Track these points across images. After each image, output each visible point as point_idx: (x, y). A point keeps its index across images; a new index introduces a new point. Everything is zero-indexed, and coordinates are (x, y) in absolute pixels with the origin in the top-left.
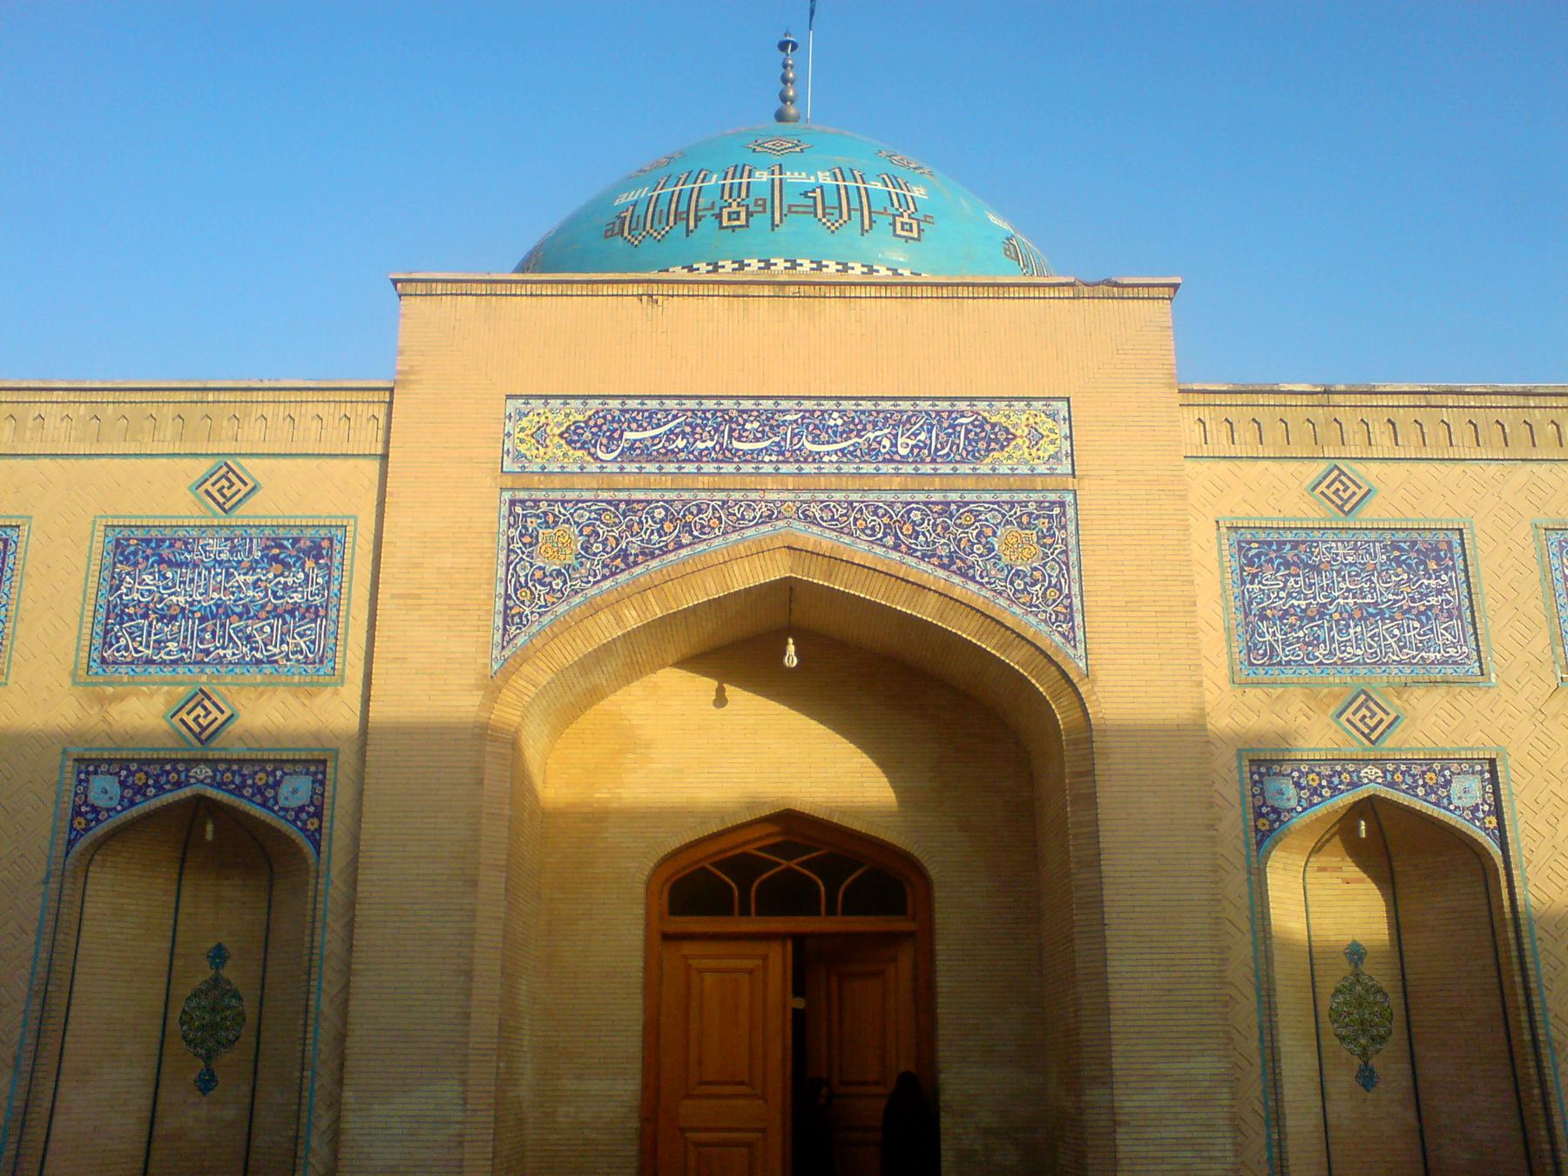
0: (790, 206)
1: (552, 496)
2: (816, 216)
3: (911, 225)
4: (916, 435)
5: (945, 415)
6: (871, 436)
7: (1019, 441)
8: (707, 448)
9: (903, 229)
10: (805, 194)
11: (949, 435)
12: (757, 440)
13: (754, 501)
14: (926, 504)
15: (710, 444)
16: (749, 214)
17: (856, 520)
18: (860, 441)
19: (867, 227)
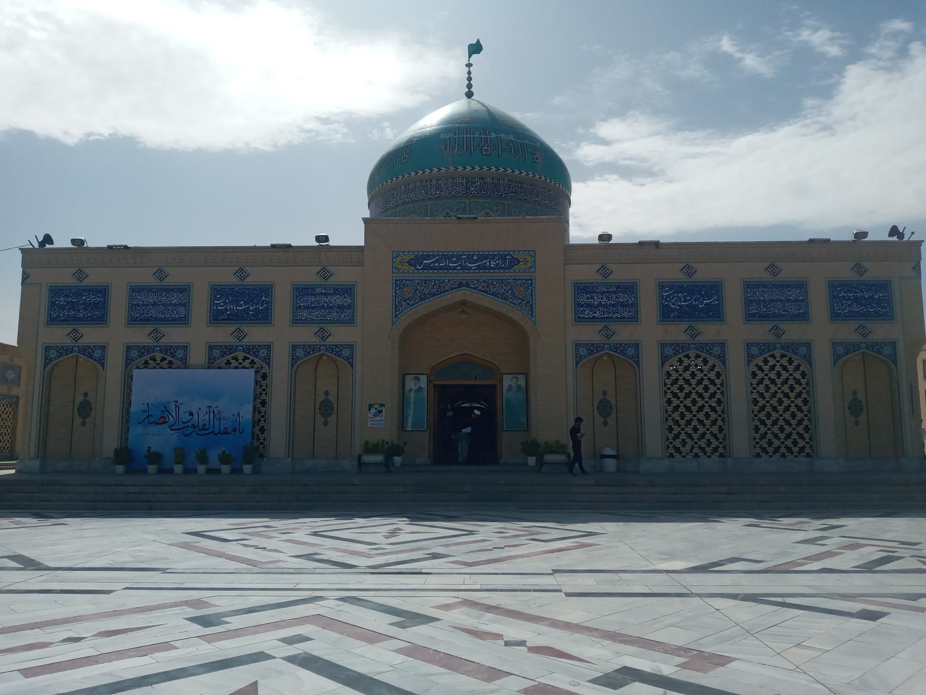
1: (406, 278)
4: (496, 261)
7: (521, 263)
14: (497, 280)
15: (444, 264)
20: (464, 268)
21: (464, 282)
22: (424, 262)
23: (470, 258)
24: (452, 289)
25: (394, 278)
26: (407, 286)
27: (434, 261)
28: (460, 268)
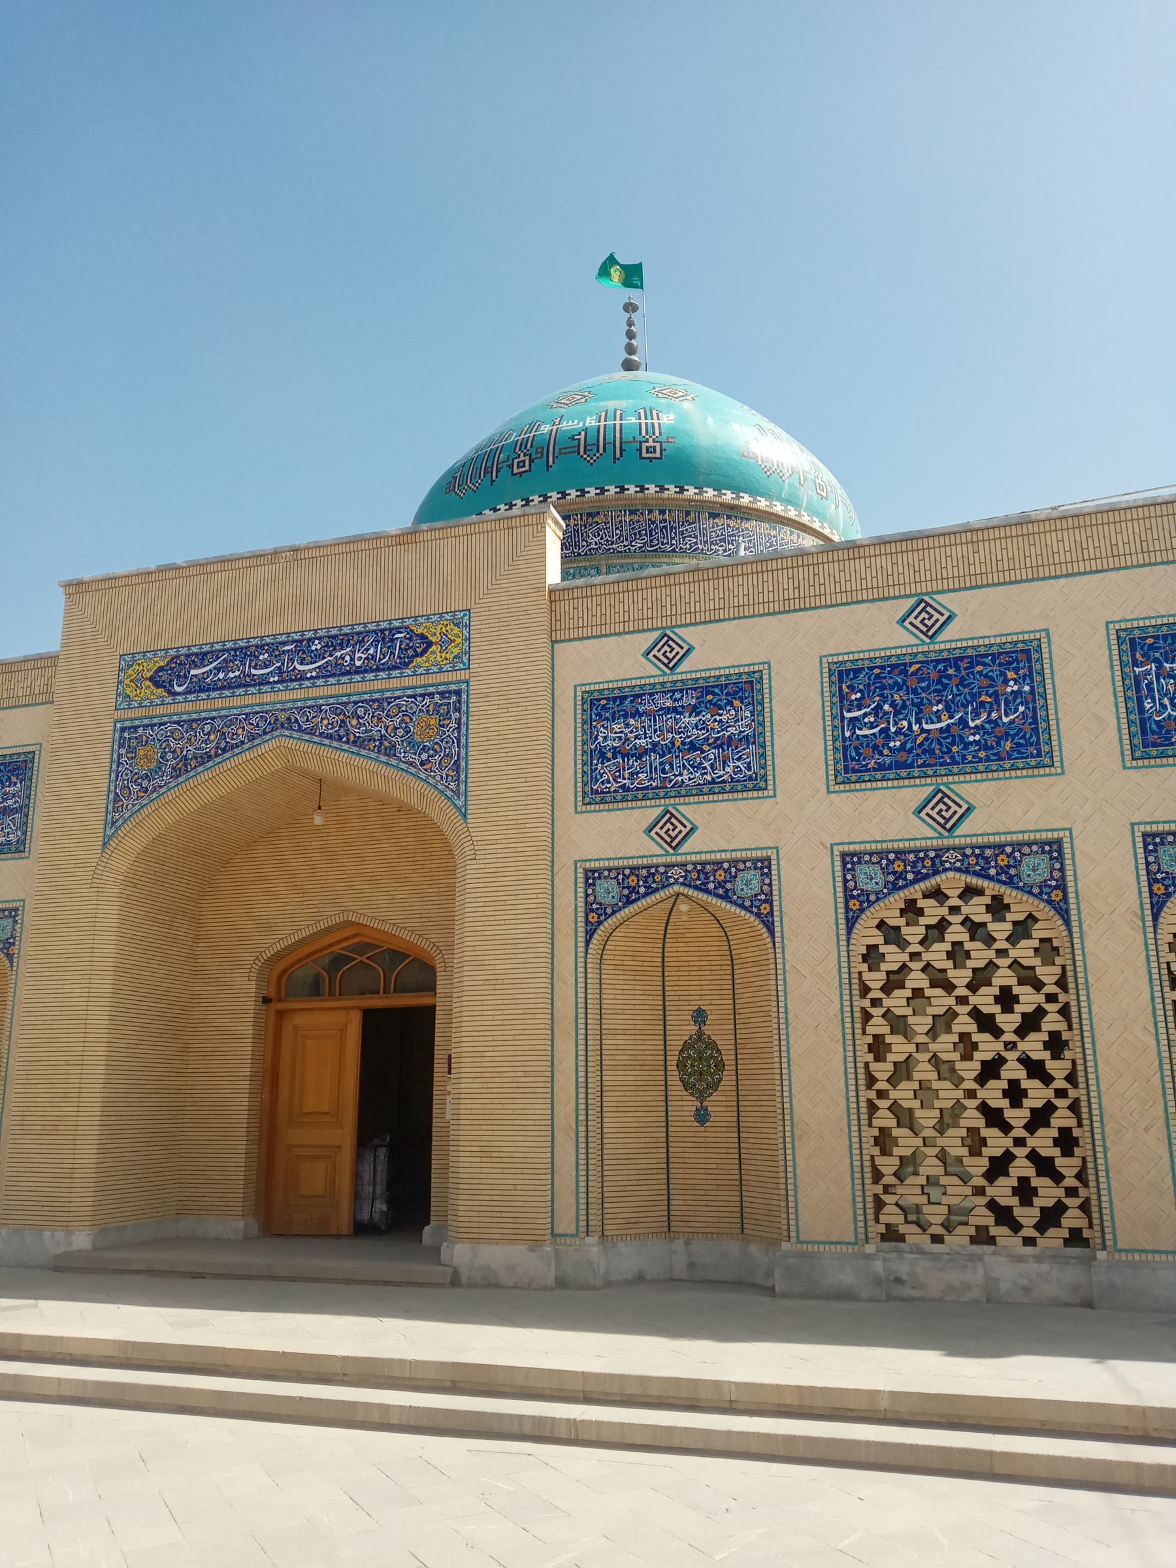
0: (560, 449)
2: (579, 454)
3: (655, 447)
4: (367, 650)
5: (387, 633)
6: (338, 654)
7: (434, 648)
8: (236, 677)
9: (647, 452)
10: (572, 438)
11: (389, 648)
12: (266, 667)
13: (266, 712)
15: (237, 673)
16: (531, 461)
17: (322, 719)
18: (331, 659)
19: (618, 455)
20: (289, 678)
21: (283, 717)
22: (193, 672)
23: (302, 647)
24: (252, 738)
25: (119, 725)
26: (147, 742)
27: (215, 668)
28: (276, 679)
